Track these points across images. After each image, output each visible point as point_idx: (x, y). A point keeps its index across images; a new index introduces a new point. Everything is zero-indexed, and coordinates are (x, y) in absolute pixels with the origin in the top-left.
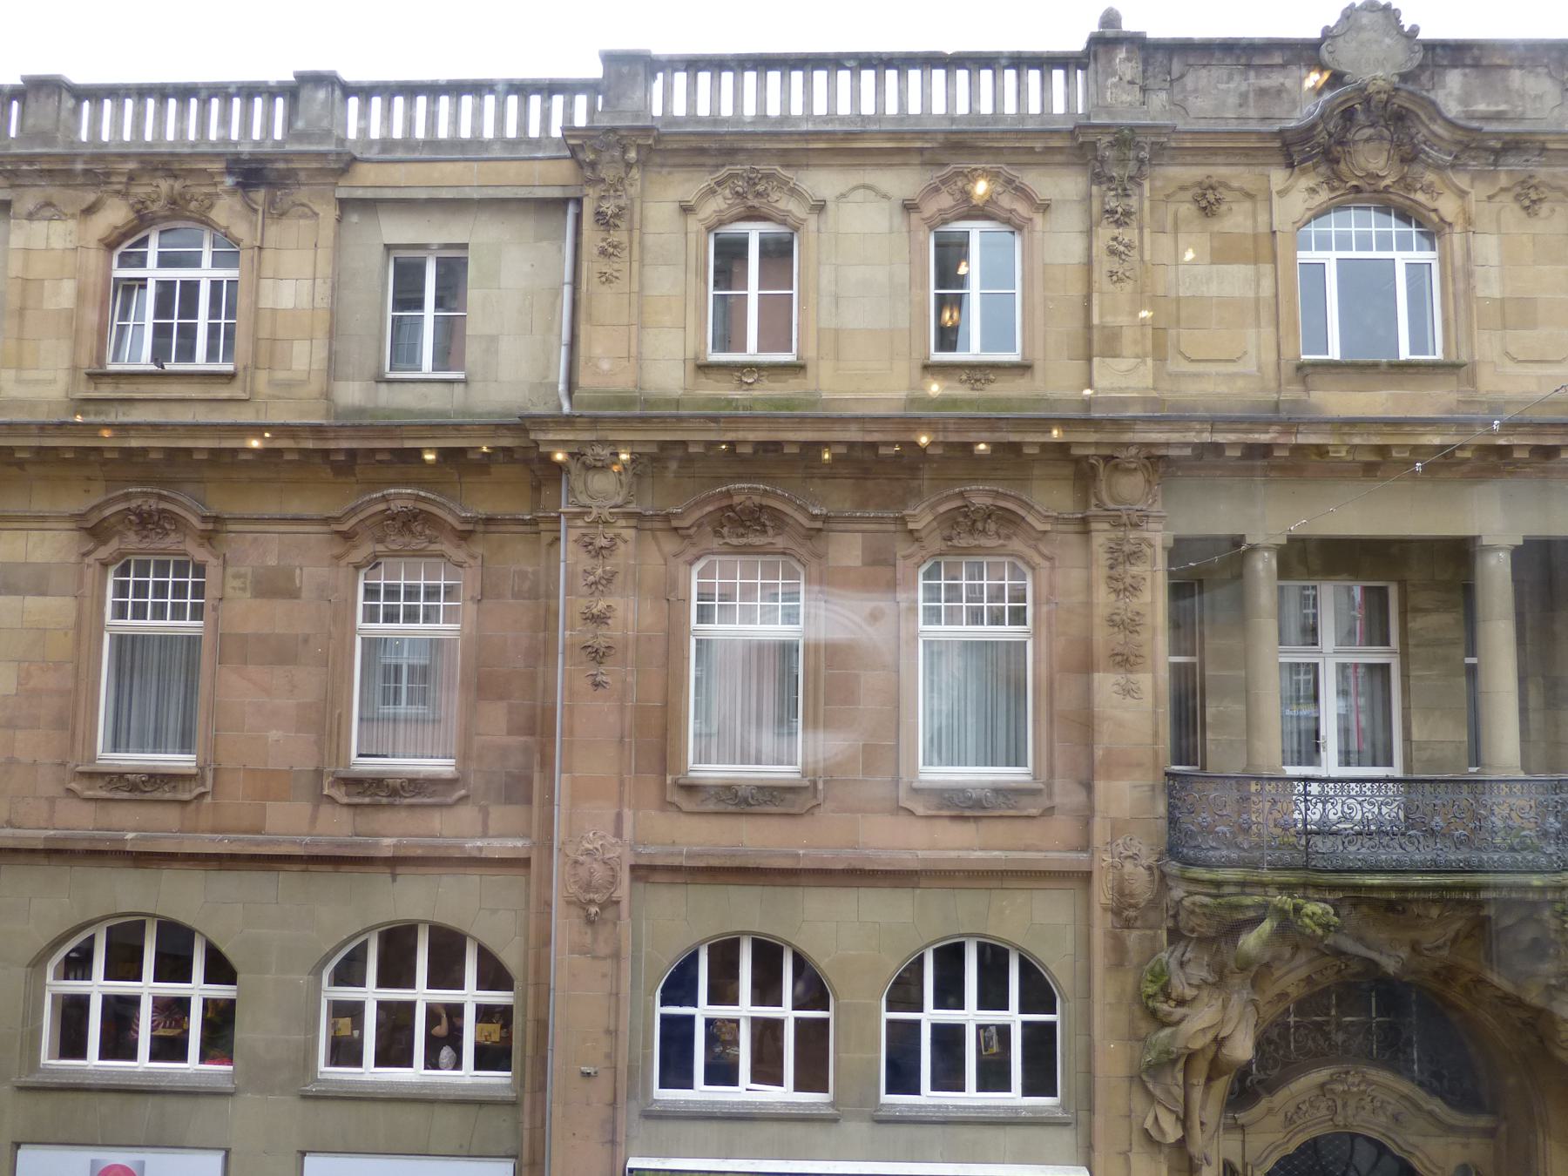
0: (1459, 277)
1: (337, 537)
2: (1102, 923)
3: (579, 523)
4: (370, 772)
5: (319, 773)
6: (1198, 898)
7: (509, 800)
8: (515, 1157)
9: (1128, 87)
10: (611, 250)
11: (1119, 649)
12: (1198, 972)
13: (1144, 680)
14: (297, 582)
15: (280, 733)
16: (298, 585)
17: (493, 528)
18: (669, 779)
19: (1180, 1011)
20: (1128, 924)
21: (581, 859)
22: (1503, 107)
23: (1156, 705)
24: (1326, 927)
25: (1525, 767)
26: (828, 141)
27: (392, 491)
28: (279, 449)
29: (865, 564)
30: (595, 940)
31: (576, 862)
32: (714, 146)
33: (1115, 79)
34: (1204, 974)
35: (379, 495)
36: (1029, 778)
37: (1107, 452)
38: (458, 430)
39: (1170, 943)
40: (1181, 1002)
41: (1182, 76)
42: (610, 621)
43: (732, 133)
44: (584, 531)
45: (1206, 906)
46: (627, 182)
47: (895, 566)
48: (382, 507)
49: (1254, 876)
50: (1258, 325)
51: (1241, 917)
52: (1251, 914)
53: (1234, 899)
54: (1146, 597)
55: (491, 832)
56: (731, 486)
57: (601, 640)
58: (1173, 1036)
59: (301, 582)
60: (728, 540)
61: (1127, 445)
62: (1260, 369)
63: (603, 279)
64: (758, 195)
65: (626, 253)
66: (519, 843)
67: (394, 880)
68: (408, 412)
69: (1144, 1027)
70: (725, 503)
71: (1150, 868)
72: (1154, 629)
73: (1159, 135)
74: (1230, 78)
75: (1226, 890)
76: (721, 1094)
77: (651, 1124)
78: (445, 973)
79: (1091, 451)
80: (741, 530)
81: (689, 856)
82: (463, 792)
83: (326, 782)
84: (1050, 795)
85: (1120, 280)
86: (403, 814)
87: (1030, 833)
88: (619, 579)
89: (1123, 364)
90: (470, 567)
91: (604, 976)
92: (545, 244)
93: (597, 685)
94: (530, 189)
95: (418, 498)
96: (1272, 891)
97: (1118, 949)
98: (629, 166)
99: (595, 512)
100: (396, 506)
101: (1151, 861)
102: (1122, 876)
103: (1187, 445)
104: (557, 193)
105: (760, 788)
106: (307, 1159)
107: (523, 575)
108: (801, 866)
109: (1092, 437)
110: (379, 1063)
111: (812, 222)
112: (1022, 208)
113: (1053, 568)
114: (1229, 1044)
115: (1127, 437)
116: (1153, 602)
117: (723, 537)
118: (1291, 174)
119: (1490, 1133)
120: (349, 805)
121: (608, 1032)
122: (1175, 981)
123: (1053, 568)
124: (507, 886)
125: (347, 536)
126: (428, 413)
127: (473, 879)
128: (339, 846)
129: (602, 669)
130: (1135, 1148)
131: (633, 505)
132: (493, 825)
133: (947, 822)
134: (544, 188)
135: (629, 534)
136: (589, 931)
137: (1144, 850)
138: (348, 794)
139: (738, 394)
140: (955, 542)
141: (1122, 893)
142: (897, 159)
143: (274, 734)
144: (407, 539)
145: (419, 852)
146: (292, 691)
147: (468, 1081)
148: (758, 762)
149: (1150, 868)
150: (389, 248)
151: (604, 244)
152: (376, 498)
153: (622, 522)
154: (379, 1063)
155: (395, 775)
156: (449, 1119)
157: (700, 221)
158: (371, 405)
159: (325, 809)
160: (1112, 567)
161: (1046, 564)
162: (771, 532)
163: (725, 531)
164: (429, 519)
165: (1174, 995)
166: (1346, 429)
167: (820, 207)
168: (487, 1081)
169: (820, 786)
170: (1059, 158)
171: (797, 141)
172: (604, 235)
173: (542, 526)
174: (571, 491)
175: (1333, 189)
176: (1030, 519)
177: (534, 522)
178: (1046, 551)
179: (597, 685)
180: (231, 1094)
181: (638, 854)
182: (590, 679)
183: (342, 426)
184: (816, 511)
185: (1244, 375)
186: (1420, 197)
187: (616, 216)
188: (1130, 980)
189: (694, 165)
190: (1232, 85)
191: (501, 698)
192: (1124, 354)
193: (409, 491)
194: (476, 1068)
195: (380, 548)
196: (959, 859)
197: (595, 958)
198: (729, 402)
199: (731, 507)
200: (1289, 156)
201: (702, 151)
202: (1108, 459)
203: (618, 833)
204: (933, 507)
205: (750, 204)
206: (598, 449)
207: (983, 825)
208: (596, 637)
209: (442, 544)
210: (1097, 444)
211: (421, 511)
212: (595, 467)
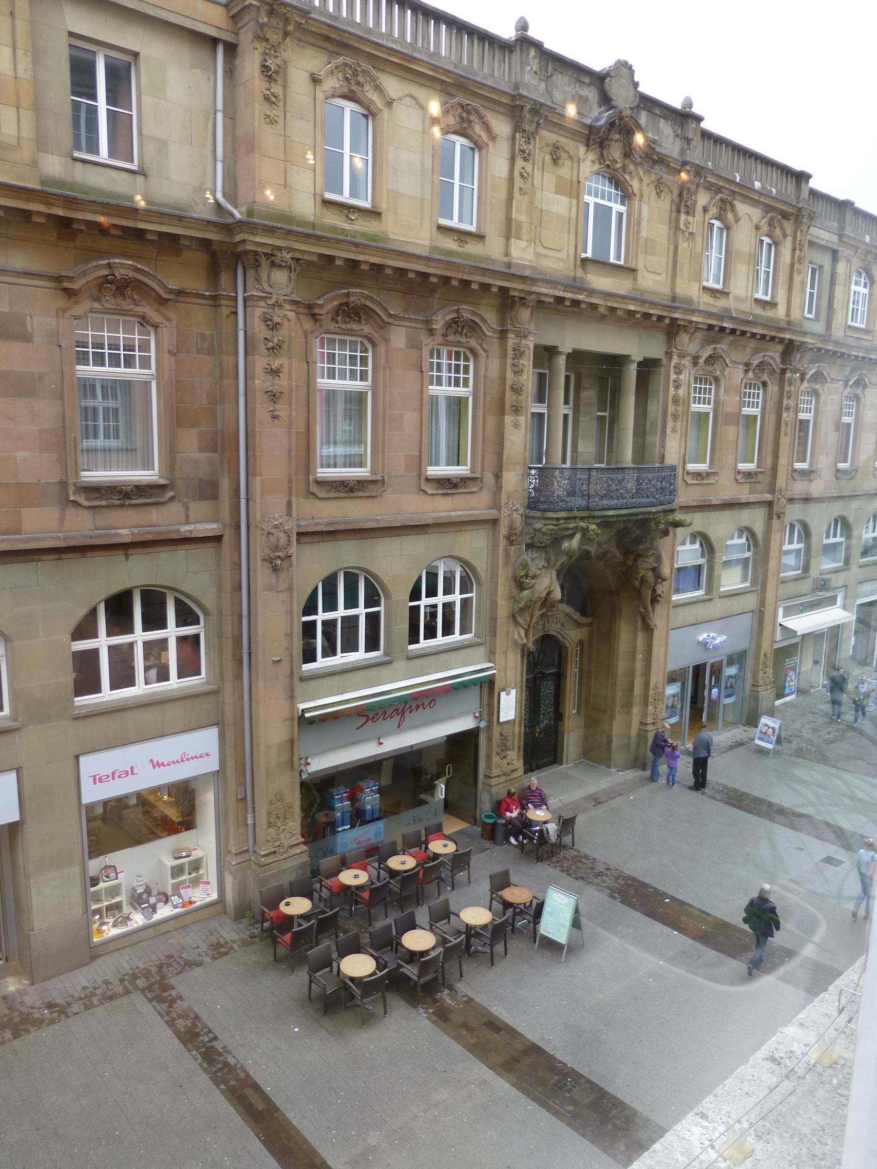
0: (633, 222)
1: (59, 293)
2: (502, 542)
3: (262, 304)
4: (105, 482)
5: (64, 485)
6: (550, 527)
7: (203, 497)
8: (217, 724)
9: (534, 75)
10: (273, 99)
11: (514, 403)
12: (542, 563)
13: (522, 419)
14: (29, 327)
15: (27, 453)
16: (30, 330)
17: (181, 299)
18: (311, 478)
19: (534, 581)
20: (511, 543)
21: (273, 531)
22: (656, 138)
23: (526, 433)
24: (597, 534)
25: (633, 462)
26: (399, 58)
27: (117, 261)
28: (29, 211)
29: (407, 347)
30: (278, 581)
31: (269, 533)
32: (337, 38)
33: (529, 68)
34: (543, 563)
35: (105, 262)
36: (469, 472)
37: (523, 295)
38: (180, 221)
39: (527, 549)
40: (534, 577)
41: (552, 75)
42: (281, 375)
43: (350, 33)
44: (265, 310)
45: (553, 530)
46: (282, 46)
47: (421, 349)
48: (105, 272)
49: (572, 514)
50: (569, 233)
51: (566, 533)
52: (571, 532)
53: (565, 526)
54: (525, 376)
55: (191, 520)
56: (350, 290)
57: (276, 387)
58: (533, 592)
59: (32, 328)
60: (340, 325)
61: (532, 293)
62: (568, 257)
63: (268, 120)
64: (358, 84)
65: (281, 104)
66: (214, 526)
67: (127, 559)
68: (101, 192)
69: (515, 592)
70: (345, 300)
71: (522, 515)
72: (528, 393)
73: (549, 111)
74: (569, 85)
75: (562, 521)
76: (431, 642)
77: (305, 684)
78: (154, 620)
79: (516, 294)
80: (347, 320)
81: (327, 524)
82: (172, 494)
83: (71, 490)
84: (482, 482)
85: (524, 194)
86: (130, 512)
87: (472, 500)
88: (285, 346)
89: (522, 244)
90: (166, 327)
91: (283, 602)
92: (198, 71)
93: (275, 417)
94: (194, 22)
95: (137, 270)
96: (578, 521)
97: (507, 556)
98: (286, 34)
99: (275, 296)
100: (119, 273)
101: (521, 512)
102: (512, 521)
103: (551, 296)
104: (213, 33)
105: (358, 482)
106: (82, 760)
107: (203, 336)
108: (380, 526)
109: (521, 286)
110: (112, 688)
111: (386, 111)
112: (484, 135)
113: (487, 357)
114: (553, 593)
115: (534, 289)
116: (528, 379)
117: (337, 322)
118: (587, 151)
119: (590, 625)
120: (89, 507)
121: (286, 635)
122: (531, 568)
123: (487, 357)
124: (202, 555)
125: (70, 293)
126: (112, 195)
127: (181, 553)
128: (91, 537)
129: (277, 406)
130: (509, 649)
131: (294, 295)
132: (192, 517)
133: (439, 497)
134: (204, 25)
135: (291, 315)
136: (274, 576)
137: (518, 506)
138: (87, 500)
139: (346, 226)
140: (448, 338)
141: (511, 528)
142: (429, 83)
143: (21, 455)
144: (119, 300)
145: (150, 537)
146: (33, 419)
147: (175, 686)
148: (335, 467)
149: (522, 515)
150: (71, 34)
151: (268, 93)
152: (102, 265)
153: (288, 307)
154: (112, 688)
155: (125, 484)
156: (174, 712)
157: (324, 92)
158: (69, 179)
159: (71, 512)
160: (513, 359)
161: (484, 354)
162: (363, 322)
163: (339, 318)
164: (140, 287)
165: (530, 575)
166: (608, 298)
167: (389, 103)
168: (161, 689)
169: (386, 479)
170: (502, 109)
171: (383, 52)
172: (266, 85)
173: (223, 302)
174: (258, 280)
175: (600, 164)
176: (484, 328)
177: (214, 298)
178: (485, 347)
179: (275, 417)
180: (17, 729)
181: (299, 526)
182: (270, 414)
183: (94, 202)
184: (392, 313)
185: (563, 260)
186: (627, 177)
187: (276, 72)
188: (510, 570)
189: (319, 47)
190: (570, 89)
191: (193, 426)
192: (523, 238)
193: (130, 263)
194: (179, 678)
195: (96, 305)
196: (448, 516)
197: (278, 592)
198: (343, 230)
199: (347, 304)
200: (588, 140)
201: (328, 39)
202: (522, 299)
203: (289, 513)
204: (445, 316)
205: (353, 88)
206: (285, 254)
207: (456, 497)
208: (273, 385)
209: (144, 307)
210: (520, 291)
211: (364, 305)
212: (280, 266)
